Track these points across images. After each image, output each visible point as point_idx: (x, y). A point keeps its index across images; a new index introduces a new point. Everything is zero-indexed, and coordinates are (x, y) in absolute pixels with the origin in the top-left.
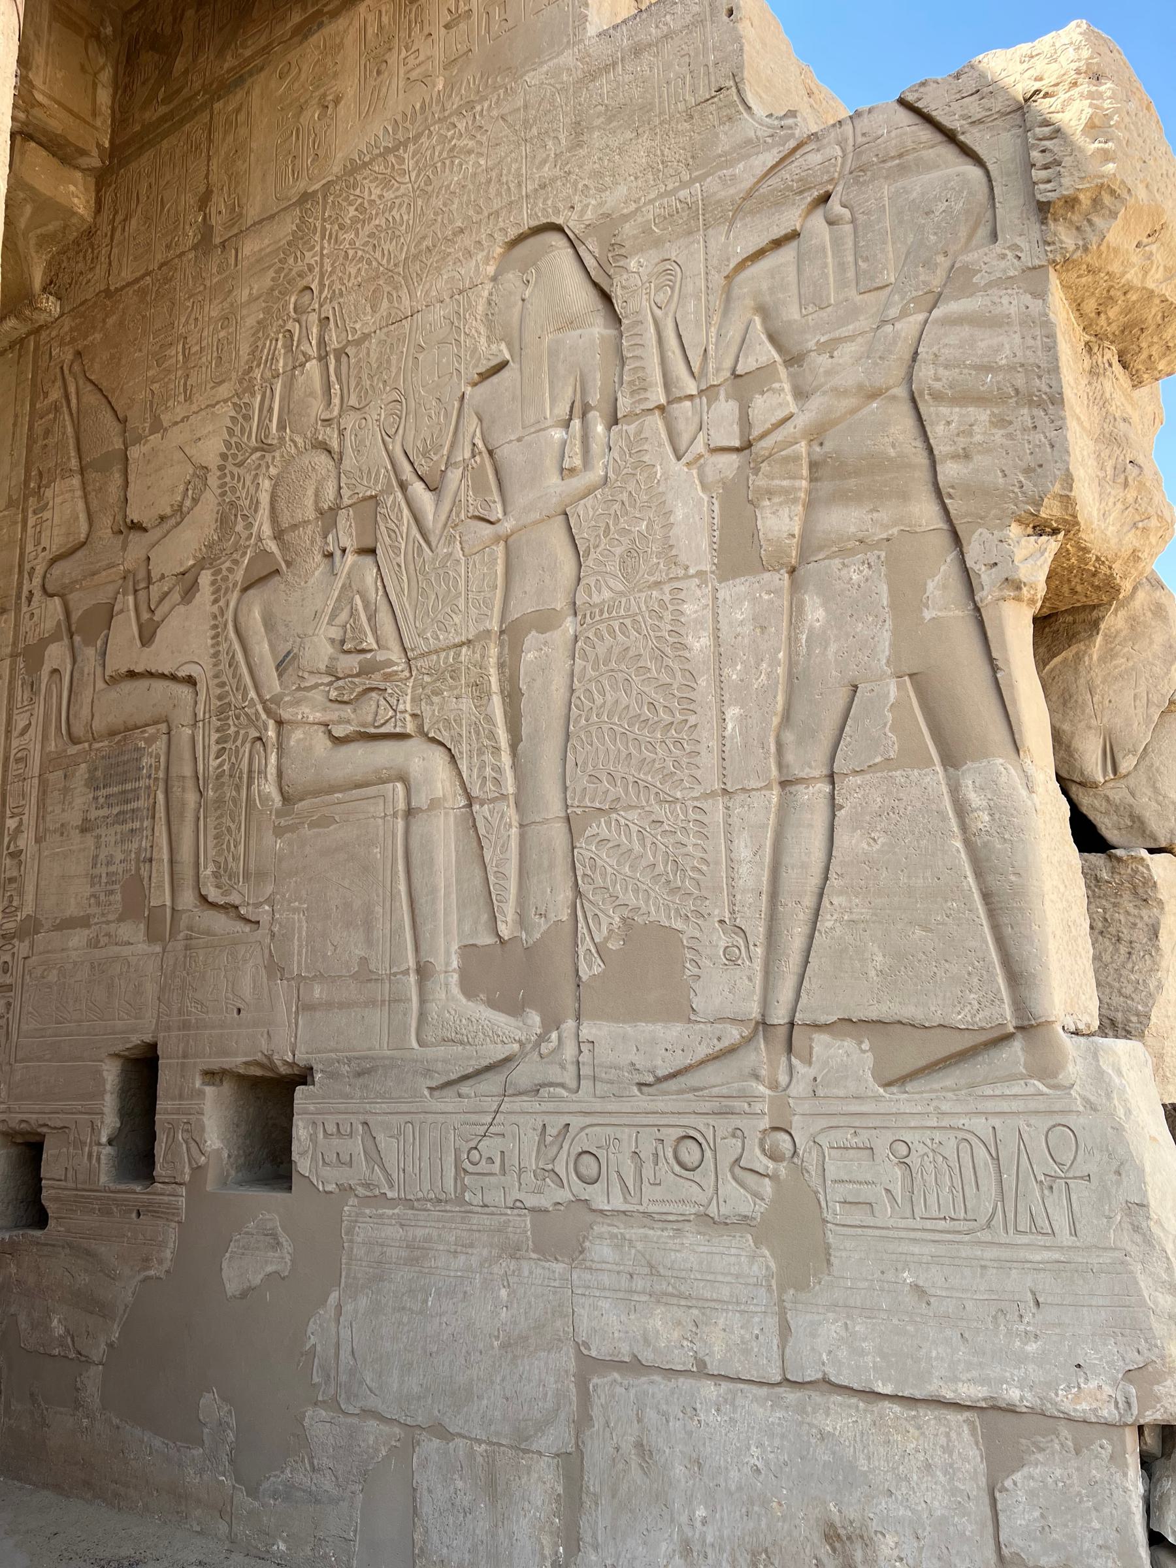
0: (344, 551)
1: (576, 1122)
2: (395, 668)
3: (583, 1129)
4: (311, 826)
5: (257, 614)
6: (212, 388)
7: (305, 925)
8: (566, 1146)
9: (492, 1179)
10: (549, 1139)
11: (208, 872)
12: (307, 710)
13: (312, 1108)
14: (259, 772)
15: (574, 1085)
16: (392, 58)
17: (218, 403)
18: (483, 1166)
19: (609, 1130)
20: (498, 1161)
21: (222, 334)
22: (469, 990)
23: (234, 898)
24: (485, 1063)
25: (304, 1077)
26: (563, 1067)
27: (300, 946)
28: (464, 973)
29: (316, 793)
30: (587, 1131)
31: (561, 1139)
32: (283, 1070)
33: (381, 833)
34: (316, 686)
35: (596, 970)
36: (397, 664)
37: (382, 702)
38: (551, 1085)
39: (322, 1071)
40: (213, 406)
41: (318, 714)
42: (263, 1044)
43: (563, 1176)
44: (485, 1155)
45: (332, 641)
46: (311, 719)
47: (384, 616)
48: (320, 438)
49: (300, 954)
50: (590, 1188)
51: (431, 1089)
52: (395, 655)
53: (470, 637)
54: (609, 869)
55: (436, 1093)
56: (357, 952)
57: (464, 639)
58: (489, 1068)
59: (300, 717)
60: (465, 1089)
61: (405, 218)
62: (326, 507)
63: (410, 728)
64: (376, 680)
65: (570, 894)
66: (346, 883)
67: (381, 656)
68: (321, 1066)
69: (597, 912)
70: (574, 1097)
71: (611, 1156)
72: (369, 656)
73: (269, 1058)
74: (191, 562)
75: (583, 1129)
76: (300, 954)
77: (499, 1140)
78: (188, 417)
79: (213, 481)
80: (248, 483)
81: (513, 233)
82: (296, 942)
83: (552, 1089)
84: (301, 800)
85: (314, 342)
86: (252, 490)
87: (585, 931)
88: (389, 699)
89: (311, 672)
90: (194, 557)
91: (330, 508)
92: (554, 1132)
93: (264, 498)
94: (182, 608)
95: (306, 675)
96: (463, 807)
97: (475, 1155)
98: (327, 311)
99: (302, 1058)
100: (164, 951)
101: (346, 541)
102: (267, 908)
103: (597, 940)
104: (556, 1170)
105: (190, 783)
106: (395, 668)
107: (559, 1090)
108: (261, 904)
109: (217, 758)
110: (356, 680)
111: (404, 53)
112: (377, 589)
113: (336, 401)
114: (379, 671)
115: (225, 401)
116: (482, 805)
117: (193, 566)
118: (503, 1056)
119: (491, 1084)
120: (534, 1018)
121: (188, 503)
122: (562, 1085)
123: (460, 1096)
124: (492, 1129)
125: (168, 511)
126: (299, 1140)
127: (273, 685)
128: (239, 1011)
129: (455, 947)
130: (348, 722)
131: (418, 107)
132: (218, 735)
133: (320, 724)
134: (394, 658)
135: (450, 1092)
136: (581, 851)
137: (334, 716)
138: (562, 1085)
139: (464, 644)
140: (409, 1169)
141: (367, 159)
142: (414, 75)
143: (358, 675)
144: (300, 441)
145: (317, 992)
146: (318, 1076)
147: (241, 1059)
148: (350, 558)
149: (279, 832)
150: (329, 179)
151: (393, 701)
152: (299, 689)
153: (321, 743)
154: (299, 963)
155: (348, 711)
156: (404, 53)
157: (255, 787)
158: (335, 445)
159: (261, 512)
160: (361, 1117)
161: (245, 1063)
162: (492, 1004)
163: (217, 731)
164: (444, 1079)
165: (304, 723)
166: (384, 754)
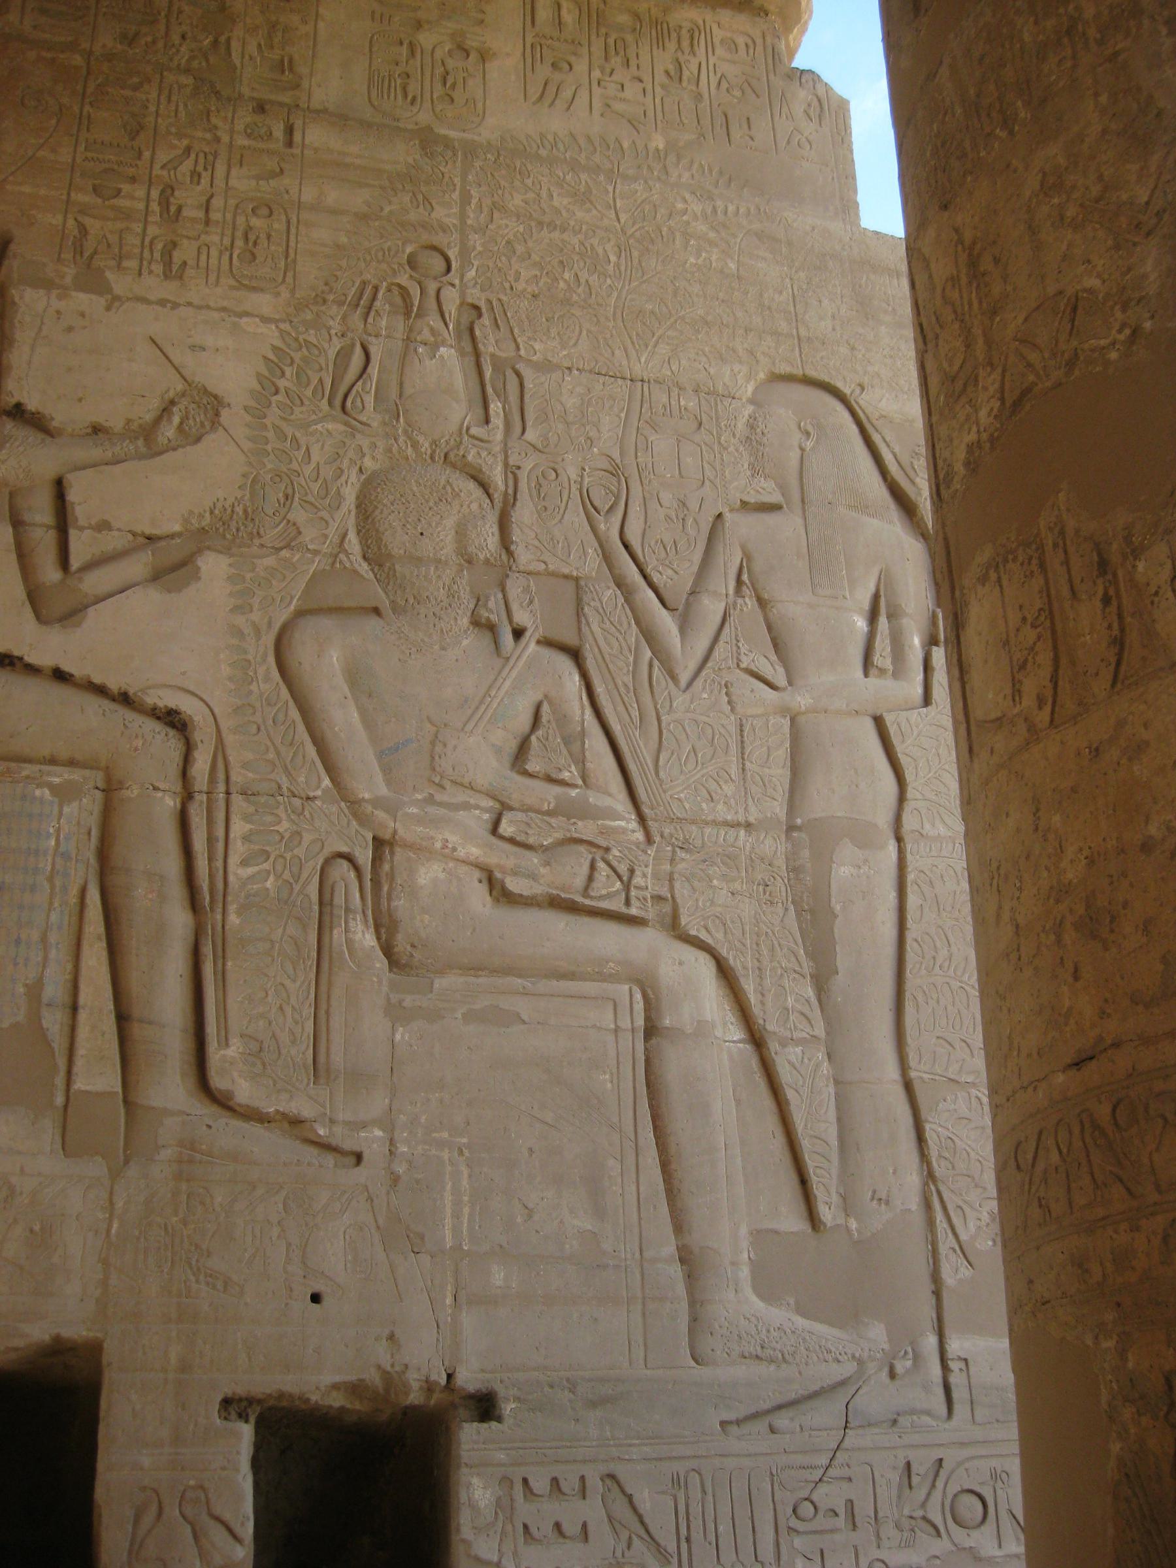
0: (518, 633)
1: (951, 1456)
2: (623, 823)
3: (959, 1464)
4: (469, 1017)
5: (335, 657)
6: (232, 288)
7: (465, 1171)
8: (940, 1484)
9: (837, 1537)
10: (915, 1480)
11: (232, 1052)
12: (453, 839)
13: (502, 1456)
14: (348, 910)
15: (943, 1410)
16: (581, 67)
17: (247, 314)
18: (821, 1522)
19: (994, 1463)
20: (841, 1511)
21: (254, 222)
22: (767, 1290)
23: (303, 1107)
24: (816, 1387)
25: (485, 1407)
26: (926, 1387)
27: (457, 1203)
28: (757, 1268)
29: (475, 969)
30: (967, 1465)
31: (931, 1478)
32: (415, 1397)
33: (612, 1053)
34: (466, 806)
35: (967, 1273)
36: (622, 819)
37: (601, 865)
38: (913, 1412)
39: (518, 1399)
40: (241, 315)
41: (474, 850)
42: (382, 1354)
43: (938, 1521)
44: (822, 1507)
45: (498, 751)
46: (461, 853)
47: (597, 743)
48: (470, 458)
49: (457, 1215)
50: (975, 1534)
51: (723, 1424)
52: (619, 801)
53: (752, 819)
54: (972, 1154)
55: (734, 1429)
56: (576, 1222)
57: (741, 819)
58: (815, 1395)
59: (438, 845)
60: (782, 1420)
61: (613, 258)
62: (482, 557)
63: (651, 913)
64: (586, 829)
65: (913, 1179)
66: (549, 1117)
67: (593, 798)
68: (514, 1392)
69: (961, 1203)
70: (946, 1426)
71: (999, 1492)
72: (574, 793)
73: (386, 1375)
74: (177, 528)
75: (959, 1464)
76: (457, 1215)
77: (845, 1485)
78: (176, 306)
79: (234, 418)
80: (315, 457)
81: (784, 368)
82: (448, 1198)
83: (915, 1417)
84: (441, 972)
85: (451, 328)
86: (327, 472)
87: (945, 1225)
88: (615, 863)
89: (454, 782)
90: (186, 521)
91: (487, 561)
92: (922, 1471)
93: (350, 495)
94: (154, 596)
95: (448, 784)
96: (740, 1041)
97: (807, 1509)
98: (476, 295)
99: (469, 1379)
100: (115, 1175)
101: (522, 617)
102: (379, 1133)
103: (963, 1237)
104: (931, 1516)
105: (176, 891)
106: (623, 823)
107: (926, 1419)
108: (364, 1126)
109: (244, 863)
110: (553, 821)
111: (596, 74)
112: (583, 708)
113: (497, 421)
114: (595, 818)
115: (266, 320)
116: (784, 1045)
117: (180, 535)
118: (839, 1378)
119: (827, 1414)
120: (877, 1333)
121: (168, 432)
122: (928, 1413)
123: (772, 1430)
124: (832, 1472)
125: (117, 424)
126: (473, 1506)
127: (370, 783)
128: (316, 1298)
129: (744, 1230)
130: (533, 877)
131: (626, 145)
132: (249, 826)
133: (478, 866)
134: (620, 808)
135: (761, 1426)
136: (934, 1126)
137: (510, 863)
138: (928, 1413)
139: (739, 825)
140: (697, 1536)
141: (543, 153)
142: (619, 107)
143: (549, 813)
144: (426, 446)
145: (498, 1276)
146: (508, 1408)
147: (328, 1379)
148: (531, 647)
149: (396, 1013)
150: (476, 138)
151: (623, 869)
152: (430, 800)
153: (478, 898)
154: (456, 1230)
155: (535, 859)
156: (596, 74)
157: (338, 935)
158: (497, 477)
159: (344, 509)
160: (604, 1469)
161: (335, 1387)
162: (801, 1311)
163: (247, 818)
164: (753, 1410)
165: (448, 854)
166: (608, 940)
